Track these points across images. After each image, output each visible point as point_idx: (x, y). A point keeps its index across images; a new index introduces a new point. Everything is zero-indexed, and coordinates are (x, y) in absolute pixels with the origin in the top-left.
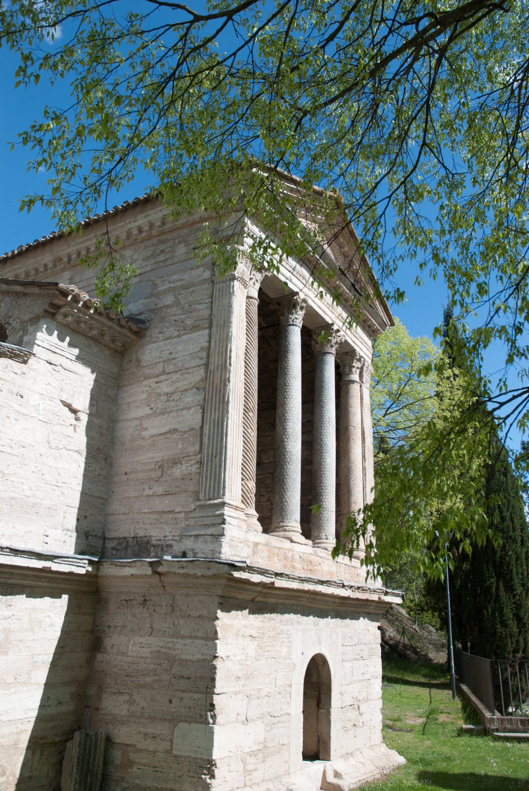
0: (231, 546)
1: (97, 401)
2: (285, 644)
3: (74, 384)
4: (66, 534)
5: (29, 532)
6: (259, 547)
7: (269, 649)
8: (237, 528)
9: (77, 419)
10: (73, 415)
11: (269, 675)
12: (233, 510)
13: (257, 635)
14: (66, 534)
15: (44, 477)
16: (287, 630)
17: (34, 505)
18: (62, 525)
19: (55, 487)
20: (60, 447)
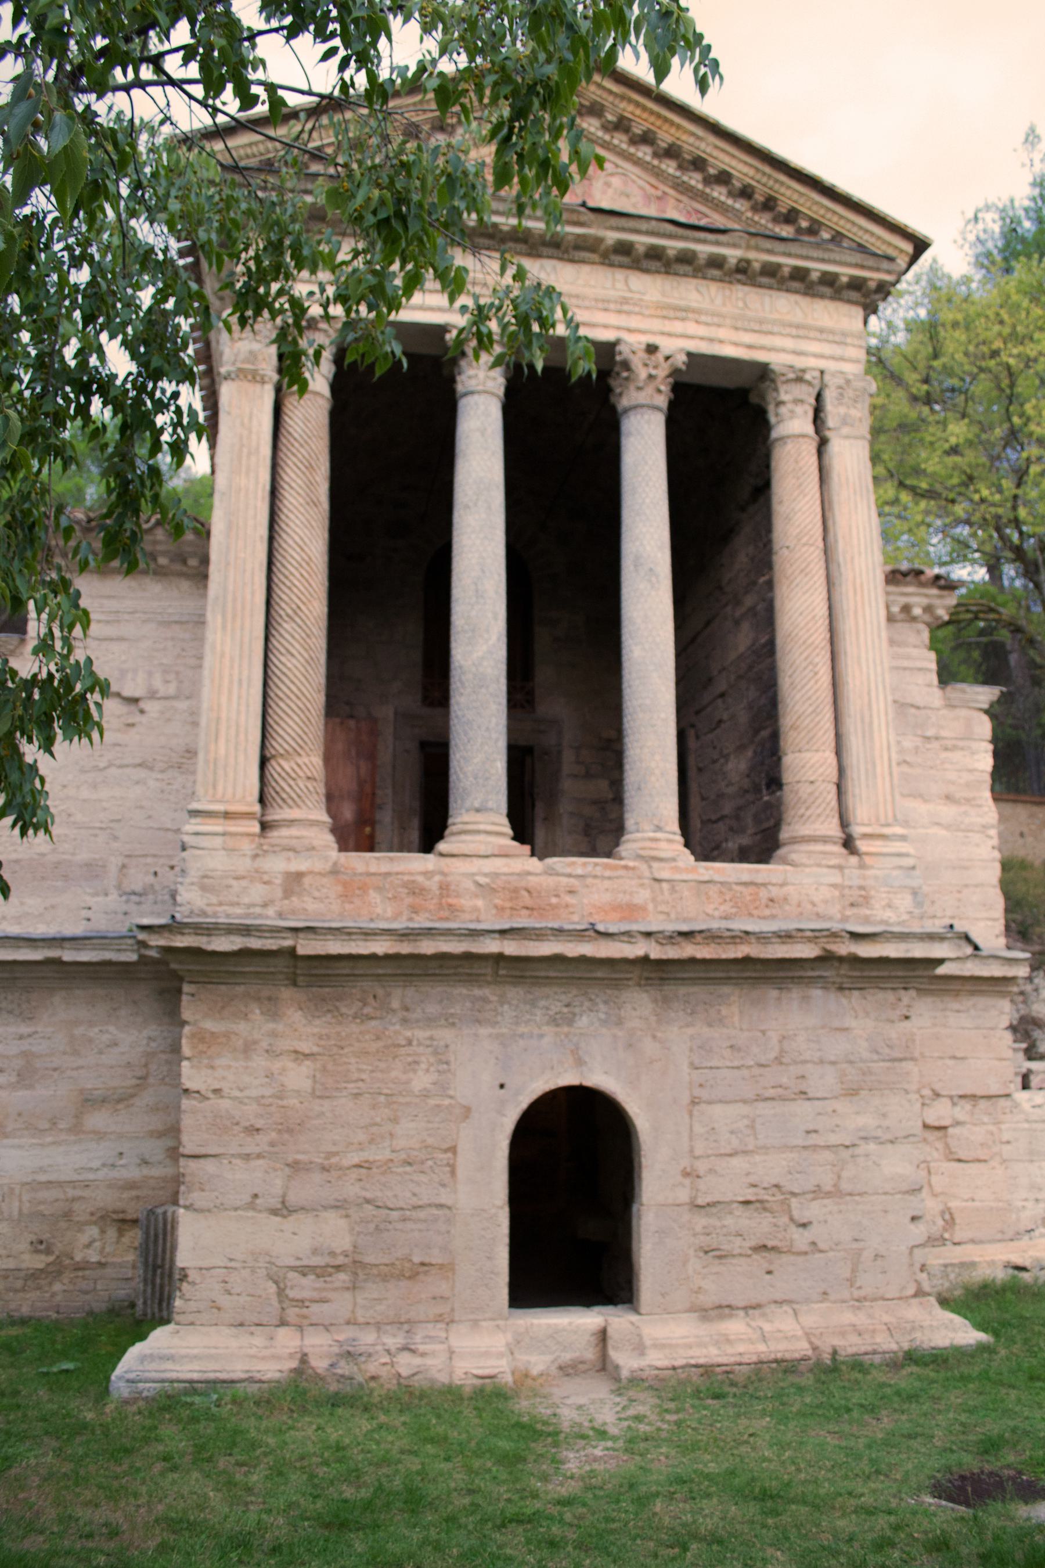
0: (204, 888)
1: (177, 673)
2: (423, 1066)
3: (123, 658)
4: (127, 901)
5: (53, 907)
6: (307, 881)
7: (364, 1076)
8: (223, 852)
9: (142, 712)
10: (133, 708)
11: (366, 1127)
12: (221, 821)
13: (315, 1049)
14: (127, 901)
15: (72, 819)
16: (431, 1038)
17: (57, 865)
18: (119, 887)
19: (97, 832)
20: (102, 765)
